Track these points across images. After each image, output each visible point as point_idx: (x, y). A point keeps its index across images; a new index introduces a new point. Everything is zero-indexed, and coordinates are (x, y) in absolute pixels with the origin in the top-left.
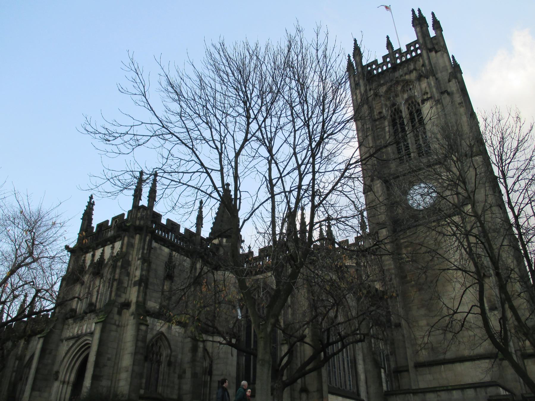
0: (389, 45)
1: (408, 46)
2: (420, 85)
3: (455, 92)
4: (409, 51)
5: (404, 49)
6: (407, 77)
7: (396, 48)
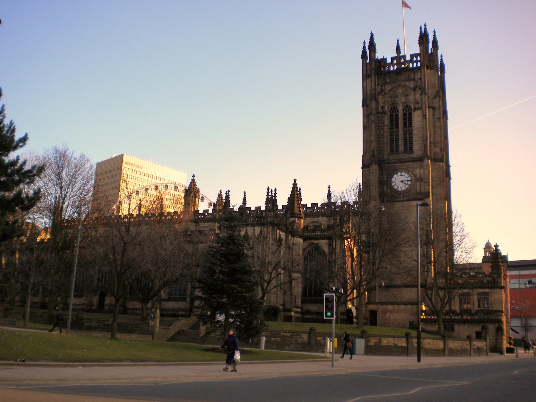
0: (398, 49)
1: (412, 56)
2: (415, 94)
3: (437, 108)
4: (411, 61)
6: (407, 84)
7: (402, 54)
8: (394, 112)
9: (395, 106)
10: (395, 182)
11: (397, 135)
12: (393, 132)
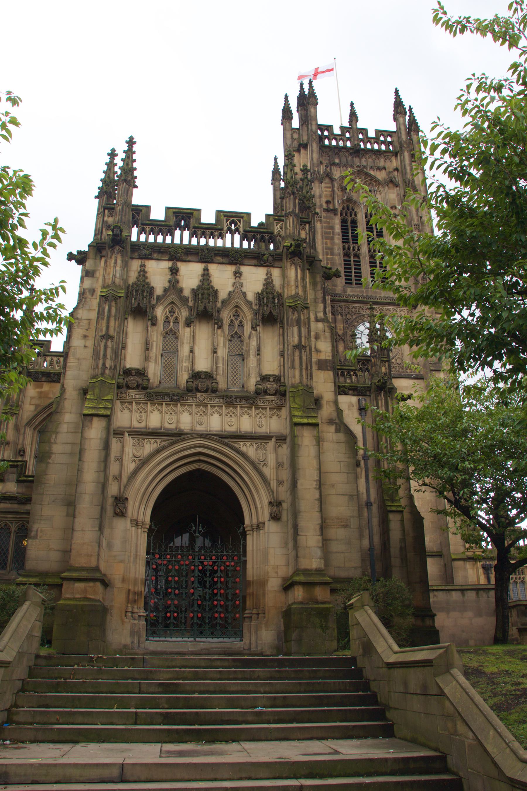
0: (353, 116)
4: (376, 140)
5: (372, 134)
6: (372, 172)
7: (360, 125)
8: (349, 215)
9: (351, 206)
10: (361, 338)
11: (357, 256)
12: (349, 249)
